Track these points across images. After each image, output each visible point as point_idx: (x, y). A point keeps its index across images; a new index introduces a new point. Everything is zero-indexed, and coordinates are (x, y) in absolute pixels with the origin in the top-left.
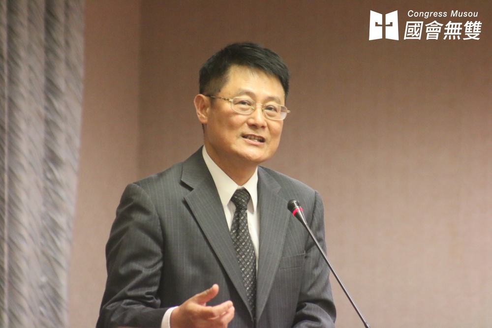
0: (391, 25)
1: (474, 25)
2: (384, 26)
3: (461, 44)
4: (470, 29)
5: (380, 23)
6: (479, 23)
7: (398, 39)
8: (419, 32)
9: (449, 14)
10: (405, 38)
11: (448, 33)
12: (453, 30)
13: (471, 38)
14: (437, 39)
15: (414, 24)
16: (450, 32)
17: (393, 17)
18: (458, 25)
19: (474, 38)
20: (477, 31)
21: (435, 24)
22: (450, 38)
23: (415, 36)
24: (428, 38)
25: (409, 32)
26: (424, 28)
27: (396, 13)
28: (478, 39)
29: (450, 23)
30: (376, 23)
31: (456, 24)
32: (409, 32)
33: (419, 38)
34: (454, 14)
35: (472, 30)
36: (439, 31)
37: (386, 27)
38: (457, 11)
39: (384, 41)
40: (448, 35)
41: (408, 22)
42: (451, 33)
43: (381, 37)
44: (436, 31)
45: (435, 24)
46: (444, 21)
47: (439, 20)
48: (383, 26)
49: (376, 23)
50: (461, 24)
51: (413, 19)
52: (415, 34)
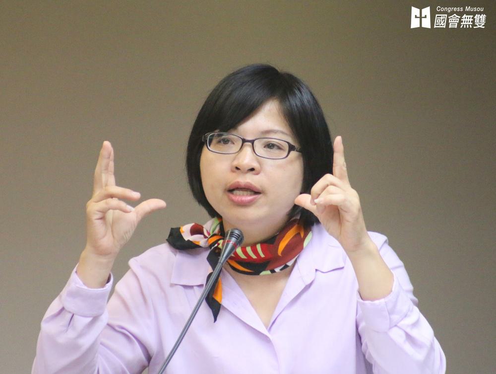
0: (425, 17)
1: (481, 17)
2: (421, 18)
3: (472, 32)
4: (478, 20)
6: (484, 16)
7: (430, 27)
8: (444, 22)
9: (464, 9)
10: (435, 27)
11: (463, 23)
12: (467, 20)
13: (479, 26)
14: (456, 27)
15: (441, 17)
17: (427, 11)
19: (481, 26)
20: (483, 22)
21: (455, 16)
22: (465, 27)
23: (441, 25)
24: (450, 27)
25: (437, 22)
27: (429, 8)
28: (484, 27)
29: (465, 16)
30: (416, 16)
31: (469, 16)
32: (437, 22)
33: (444, 27)
34: (468, 9)
35: (480, 21)
36: (458, 22)
38: (469, 7)
39: (421, 29)
40: (464, 25)
41: (437, 15)
42: (466, 23)
43: (419, 26)
44: (456, 21)
45: (455, 16)
46: (461, 14)
47: (458, 13)
48: (420, 18)
49: (416, 16)
50: (472, 16)
52: (442, 24)
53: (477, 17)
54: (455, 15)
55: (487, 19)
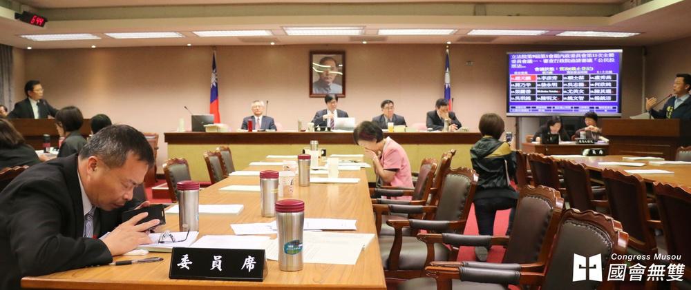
0: (595, 267)
1: (678, 267)
2: (588, 268)
4: (673, 271)
5: (584, 265)
6: (683, 265)
8: (622, 274)
10: (609, 279)
11: (651, 275)
12: (656, 272)
13: (674, 279)
14: (640, 280)
15: (617, 267)
16: (653, 273)
18: (661, 269)
19: (677, 279)
20: (681, 273)
22: (653, 280)
23: (618, 278)
24: (631, 280)
26: (628, 270)
27: (599, 256)
28: (681, 280)
29: (653, 265)
31: (659, 266)
33: (623, 280)
35: (676, 272)
36: (643, 273)
37: (590, 269)
39: (588, 283)
40: (652, 277)
41: (611, 265)
42: (655, 275)
43: (585, 279)
44: (640, 273)
47: (642, 262)
51: (617, 262)
52: (619, 275)
53: (671, 267)
54: (639, 264)
55: (685, 271)
